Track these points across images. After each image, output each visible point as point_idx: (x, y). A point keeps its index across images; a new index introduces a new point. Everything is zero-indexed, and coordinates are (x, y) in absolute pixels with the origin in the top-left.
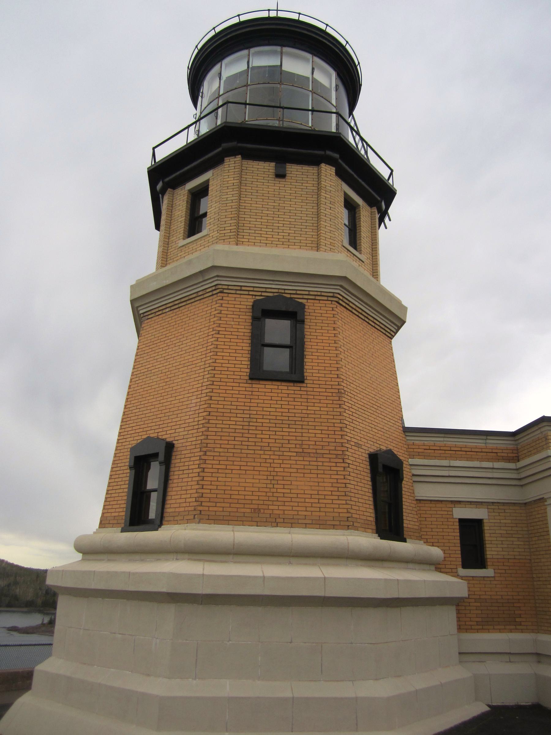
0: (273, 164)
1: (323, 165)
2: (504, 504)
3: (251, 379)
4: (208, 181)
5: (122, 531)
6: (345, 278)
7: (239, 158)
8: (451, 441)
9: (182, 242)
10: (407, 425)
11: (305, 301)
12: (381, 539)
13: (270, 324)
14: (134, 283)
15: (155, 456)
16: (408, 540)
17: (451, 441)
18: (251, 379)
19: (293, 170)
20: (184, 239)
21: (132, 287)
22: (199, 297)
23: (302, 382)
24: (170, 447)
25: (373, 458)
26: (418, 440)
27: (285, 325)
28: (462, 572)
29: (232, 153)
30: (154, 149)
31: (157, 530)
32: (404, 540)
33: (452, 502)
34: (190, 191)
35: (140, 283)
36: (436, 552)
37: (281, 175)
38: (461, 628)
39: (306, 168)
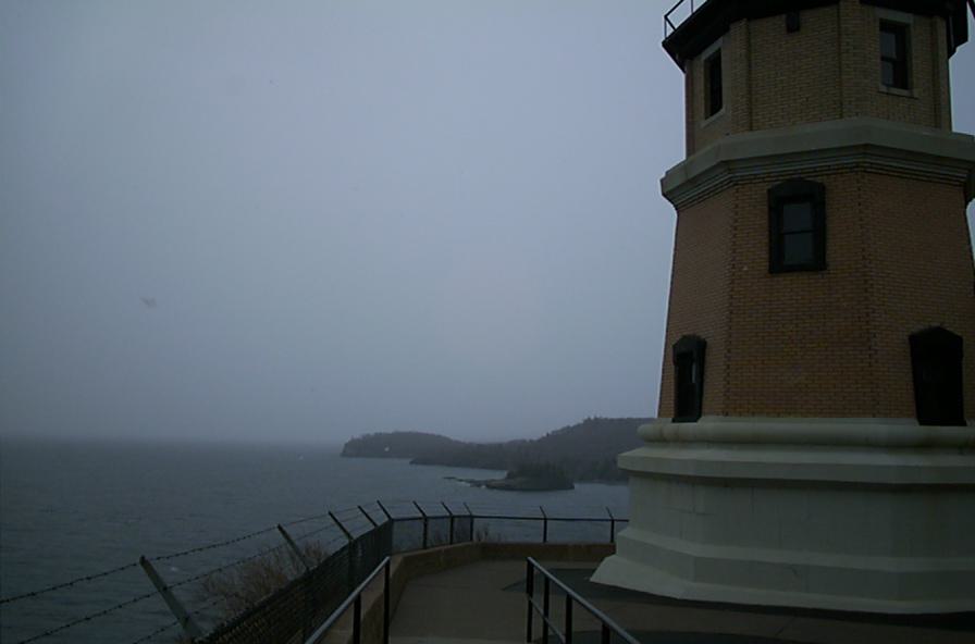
0: (784, 16)
4: (720, 49)
5: (674, 421)
7: (743, 23)
9: (704, 123)
11: (825, 177)
12: (922, 423)
14: (663, 175)
19: (809, 18)
20: (706, 118)
21: (662, 181)
23: (825, 269)
25: (915, 340)
30: (666, 17)
31: (695, 421)
32: (964, 424)
34: (706, 61)
37: (793, 28)
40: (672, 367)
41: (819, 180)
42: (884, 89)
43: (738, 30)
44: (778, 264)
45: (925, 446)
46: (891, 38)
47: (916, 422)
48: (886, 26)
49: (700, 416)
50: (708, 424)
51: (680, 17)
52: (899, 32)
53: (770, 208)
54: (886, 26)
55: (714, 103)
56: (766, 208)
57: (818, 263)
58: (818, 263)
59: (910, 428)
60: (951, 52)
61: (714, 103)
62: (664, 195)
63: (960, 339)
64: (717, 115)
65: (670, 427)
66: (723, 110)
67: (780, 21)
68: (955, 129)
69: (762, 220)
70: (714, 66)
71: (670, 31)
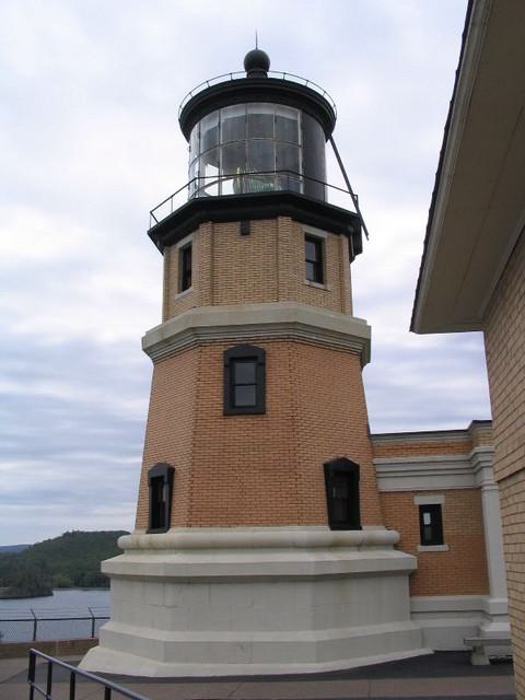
0: (239, 223)
1: (280, 219)
2: (459, 490)
3: (225, 415)
4: (190, 243)
5: (147, 533)
6: (295, 323)
8: (410, 441)
9: (177, 296)
10: (372, 433)
12: (332, 529)
13: (239, 366)
15: (162, 477)
16: (364, 527)
17: (410, 441)
18: (225, 415)
19: (257, 226)
22: (185, 349)
23: (264, 413)
24: (171, 471)
25: (326, 467)
26: (382, 443)
27: (250, 367)
28: (421, 548)
29: (204, 220)
32: (361, 529)
33: (413, 492)
35: (149, 334)
36: (394, 535)
37: (245, 233)
38: (411, 595)
39: (266, 222)
40: (147, 490)
41: (261, 346)
42: (307, 282)
43: (205, 229)
44: (231, 409)
45: (335, 546)
46: (312, 246)
47: (327, 527)
48: (309, 238)
49: (169, 528)
50: (175, 534)
51: (163, 214)
52: (318, 243)
53: (225, 366)
54: (309, 238)
55: (186, 282)
56: (222, 365)
57: (258, 409)
58: (258, 409)
59: (324, 533)
60: (352, 259)
61: (186, 282)
62: (145, 350)
63: (357, 467)
64: (187, 291)
65: (145, 538)
66: (191, 289)
67: (236, 226)
68: (354, 315)
69: (217, 373)
70: (187, 253)
71: (154, 224)
